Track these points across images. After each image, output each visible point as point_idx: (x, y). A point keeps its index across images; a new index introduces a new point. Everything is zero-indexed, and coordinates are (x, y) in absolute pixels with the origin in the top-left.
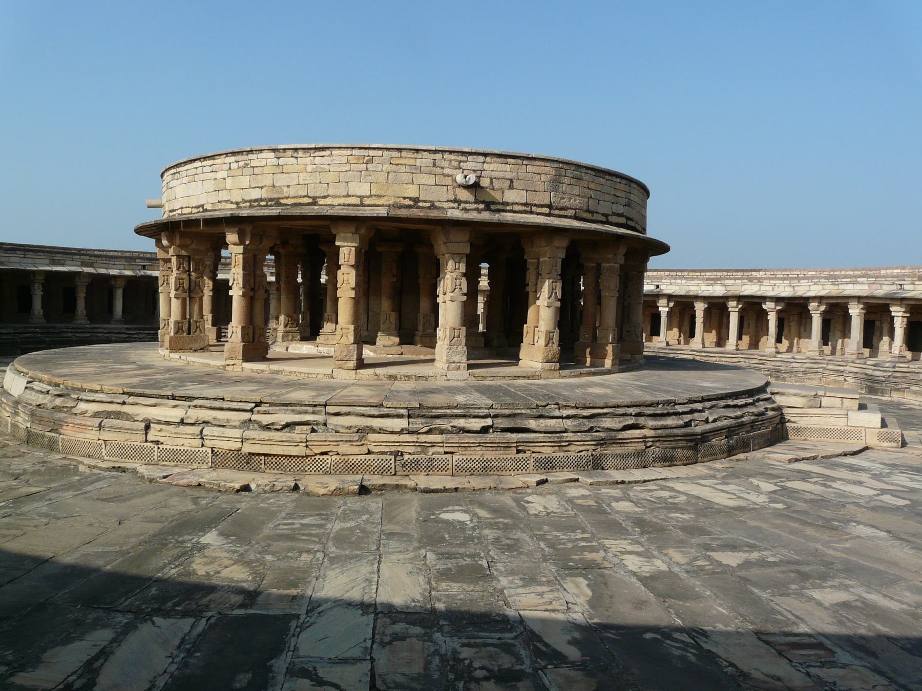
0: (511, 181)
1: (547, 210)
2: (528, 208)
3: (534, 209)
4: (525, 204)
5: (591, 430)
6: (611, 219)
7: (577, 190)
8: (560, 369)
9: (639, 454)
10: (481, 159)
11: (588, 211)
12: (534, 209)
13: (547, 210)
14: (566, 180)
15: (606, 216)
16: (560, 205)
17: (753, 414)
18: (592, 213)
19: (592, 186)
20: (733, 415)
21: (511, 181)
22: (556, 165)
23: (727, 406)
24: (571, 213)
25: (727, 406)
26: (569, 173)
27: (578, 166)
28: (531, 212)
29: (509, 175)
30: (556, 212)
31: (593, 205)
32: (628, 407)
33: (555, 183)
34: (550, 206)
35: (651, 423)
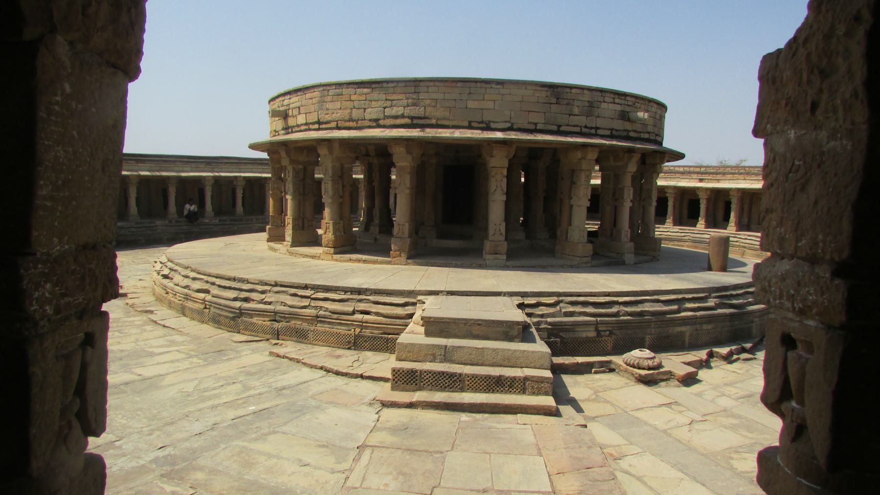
0: (299, 108)
1: (316, 126)
2: (308, 127)
3: (311, 126)
4: (306, 124)
5: (186, 287)
6: (381, 122)
7: (338, 105)
8: (335, 253)
9: (200, 313)
10: (289, 97)
11: (351, 120)
12: (311, 126)
13: (316, 126)
14: (329, 98)
15: (377, 120)
16: (325, 121)
17: (327, 310)
18: (357, 121)
19: (353, 98)
20: (290, 303)
21: (299, 108)
22: (321, 89)
23: (295, 295)
24: (333, 125)
25: (295, 295)
26: (331, 92)
27: (339, 85)
28: (309, 130)
29: (298, 104)
30: (324, 126)
31: (356, 114)
32: (217, 277)
33: (322, 102)
34: (319, 122)
35: (215, 291)
